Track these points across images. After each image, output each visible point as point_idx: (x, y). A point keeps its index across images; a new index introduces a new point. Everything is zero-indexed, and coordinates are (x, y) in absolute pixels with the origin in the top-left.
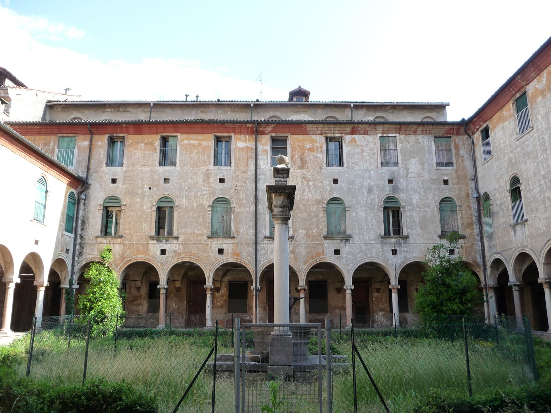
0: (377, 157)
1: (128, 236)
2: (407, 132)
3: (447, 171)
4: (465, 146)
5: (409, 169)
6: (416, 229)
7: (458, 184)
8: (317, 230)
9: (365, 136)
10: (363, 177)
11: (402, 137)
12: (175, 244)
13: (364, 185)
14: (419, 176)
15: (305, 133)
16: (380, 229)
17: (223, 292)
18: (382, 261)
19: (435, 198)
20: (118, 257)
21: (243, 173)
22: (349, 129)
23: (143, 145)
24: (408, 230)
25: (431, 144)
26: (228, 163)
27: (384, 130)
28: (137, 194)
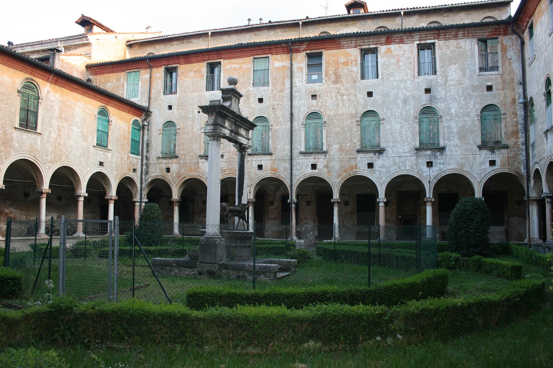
0: (414, 66)
1: (182, 156)
2: (447, 36)
4: (514, 47)
5: (448, 76)
6: (453, 140)
7: (503, 89)
8: (351, 145)
9: (401, 45)
10: (398, 88)
11: (442, 42)
13: (400, 96)
14: (459, 84)
15: (340, 47)
16: (415, 141)
17: (276, 205)
18: (416, 174)
19: (476, 106)
20: (175, 175)
21: (279, 91)
22: (383, 40)
23: (192, 73)
24: (445, 141)
25: (474, 47)
26: (266, 84)
27: (421, 37)
28: (188, 118)
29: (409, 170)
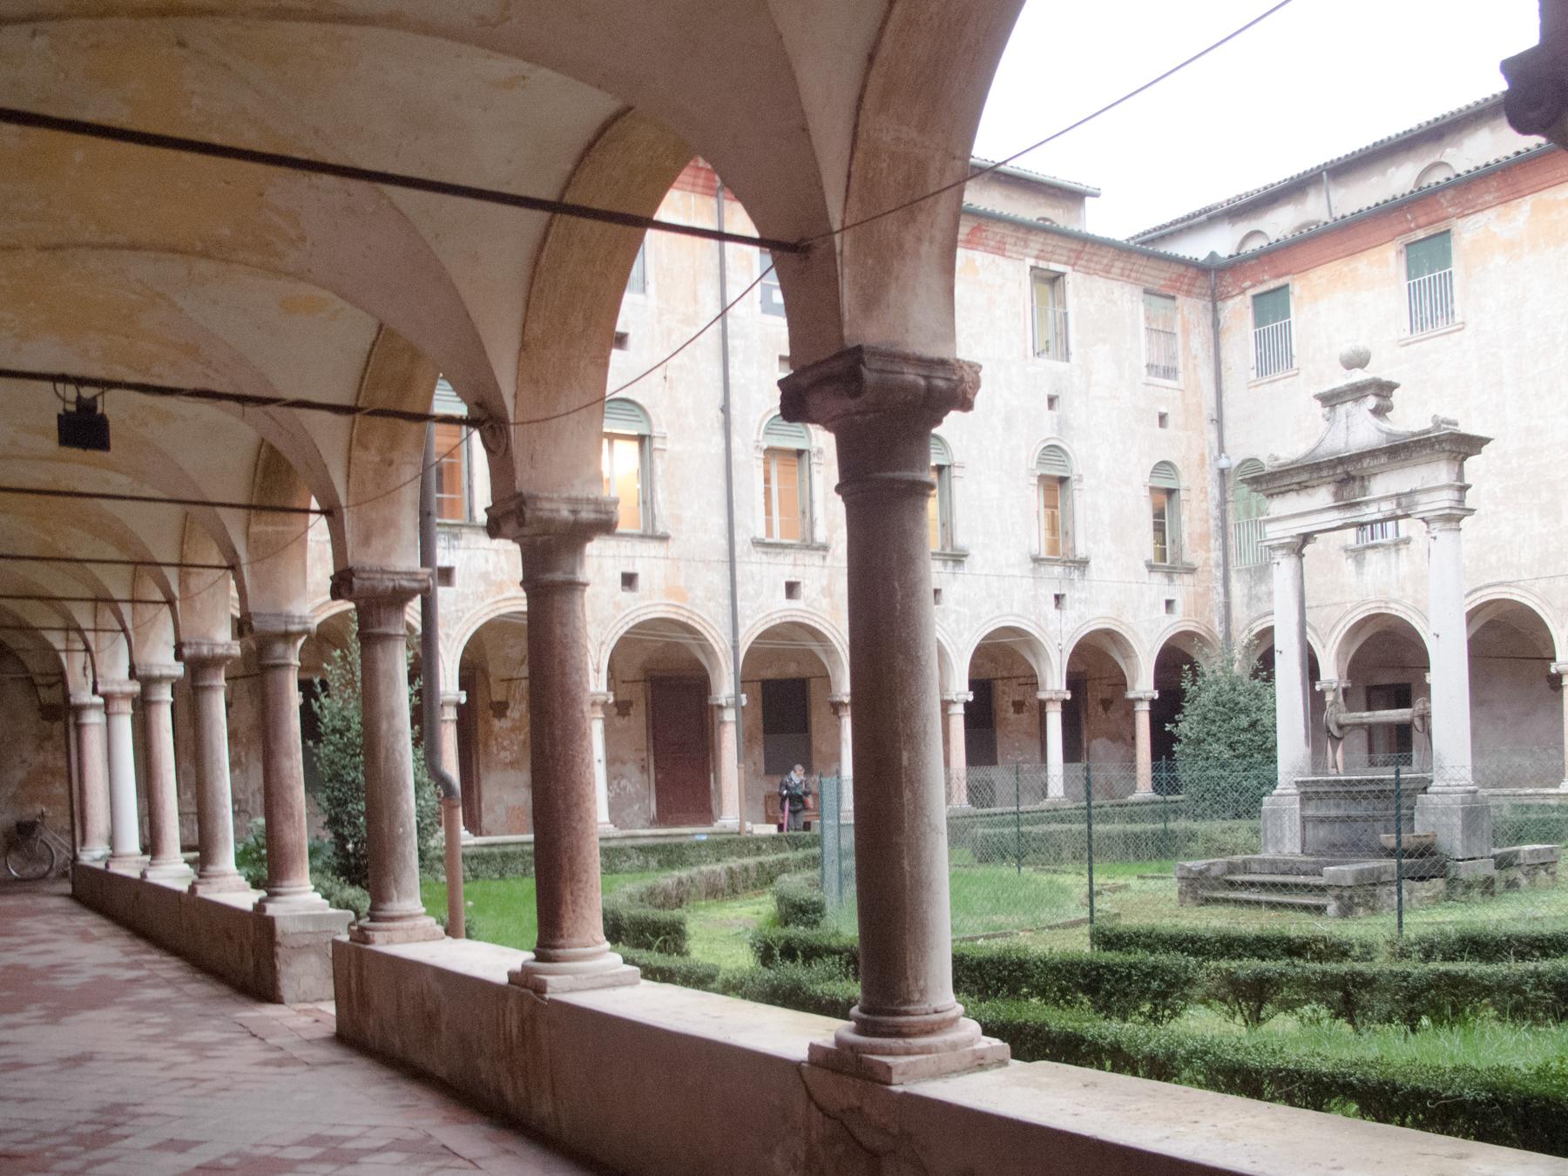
2: (1092, 265)
3: (1165, 390)
11: (1079, 275)
12: (483, 552)
17: (517, 715)
18: (1034, 626)
27: (1042, 251)
29: (1018, 616)
